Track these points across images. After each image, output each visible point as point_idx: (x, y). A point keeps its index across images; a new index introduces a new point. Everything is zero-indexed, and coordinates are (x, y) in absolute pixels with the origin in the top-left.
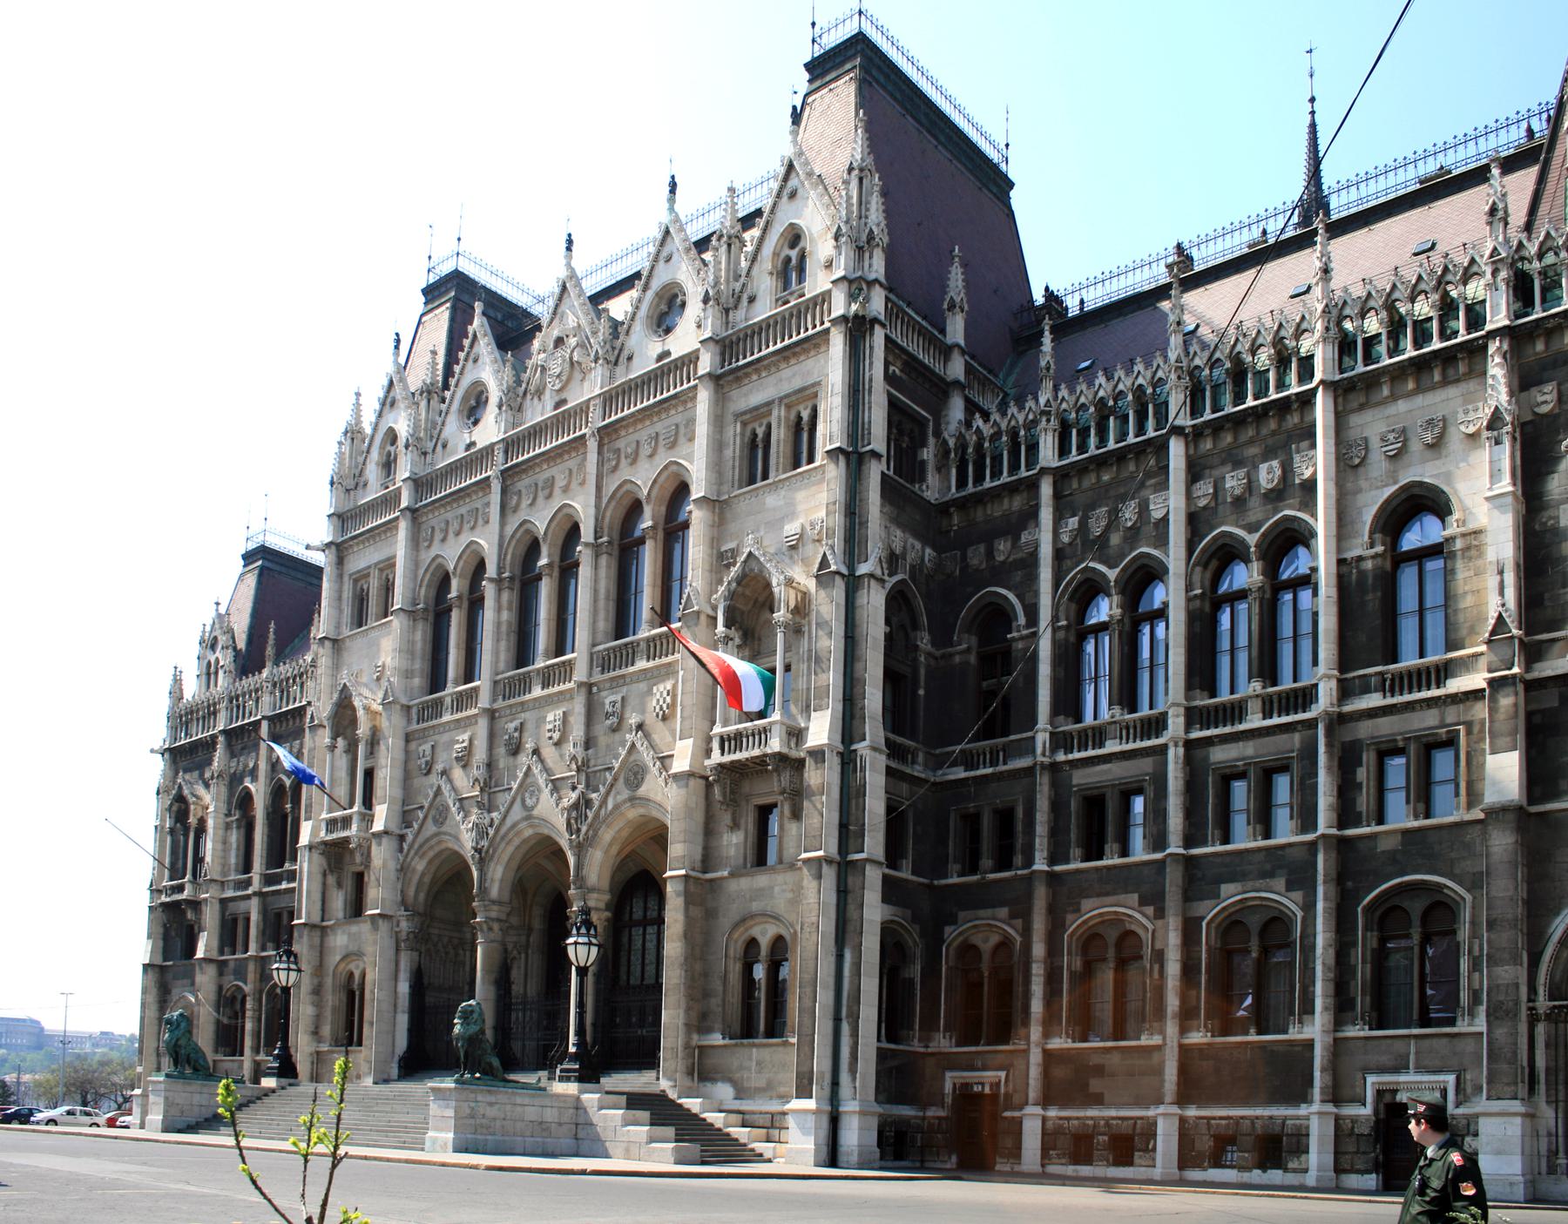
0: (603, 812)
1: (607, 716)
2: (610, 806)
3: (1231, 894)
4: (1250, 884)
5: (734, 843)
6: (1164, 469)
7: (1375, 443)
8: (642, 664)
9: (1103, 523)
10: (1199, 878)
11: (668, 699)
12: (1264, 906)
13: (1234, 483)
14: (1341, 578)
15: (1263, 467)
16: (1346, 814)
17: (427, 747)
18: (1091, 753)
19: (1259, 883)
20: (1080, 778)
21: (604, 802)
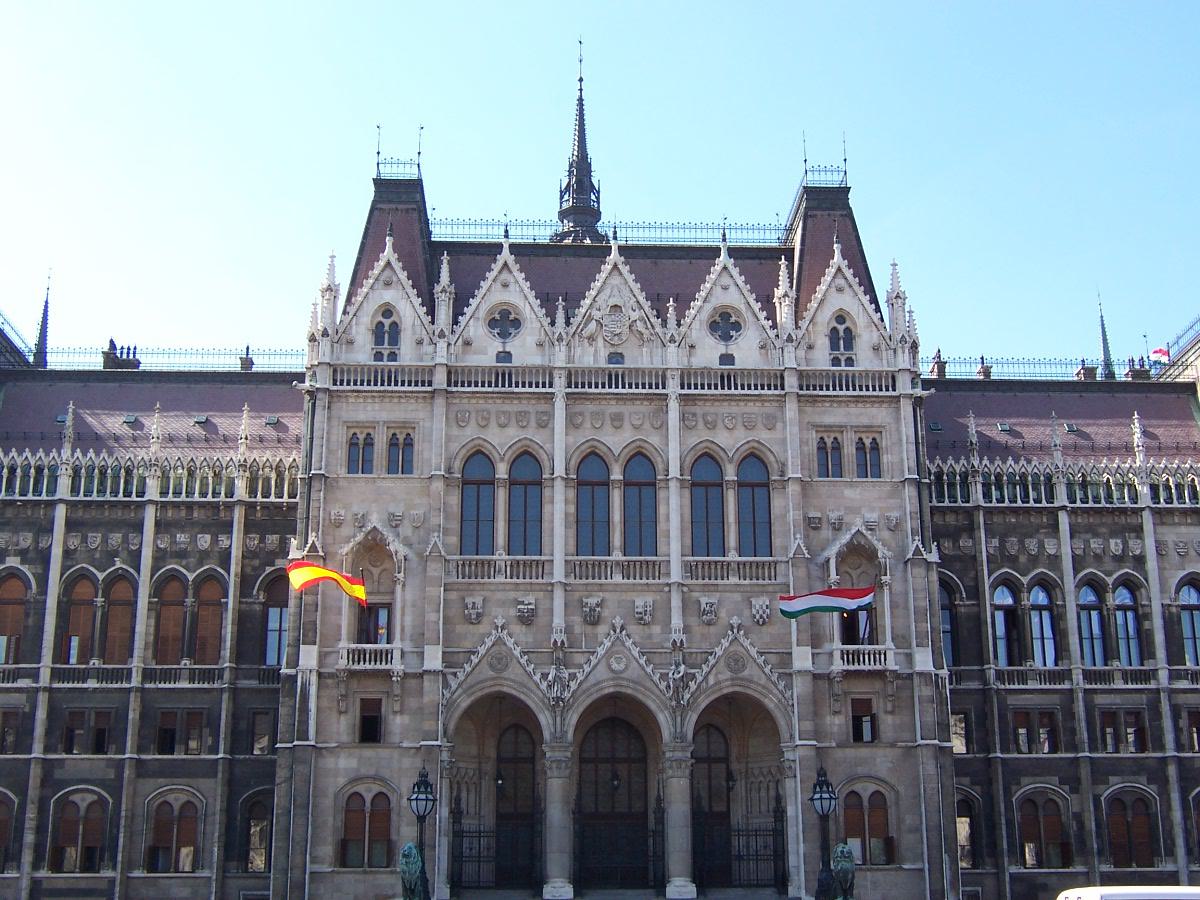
0: (704, 684)
1: (705, 613)
2: (711, 681)
3: (1116, 784)
4: (1126, 778)
5: (838, 723)
6: (1054, 527)
7: (1171, 545)
8: (734, 580)
9: (1016, 548)
10: (1101, 771)
11: (768, 611)
12: (1134, 791)
13: (1097, 546)
14: (1163, 613)
15: (1112, 542)
16: (1179, 747)
17: (479, 600)
18: (1016, 687)
19: (1132, 778)
20: (1012, 700)
21: (706, 678)
